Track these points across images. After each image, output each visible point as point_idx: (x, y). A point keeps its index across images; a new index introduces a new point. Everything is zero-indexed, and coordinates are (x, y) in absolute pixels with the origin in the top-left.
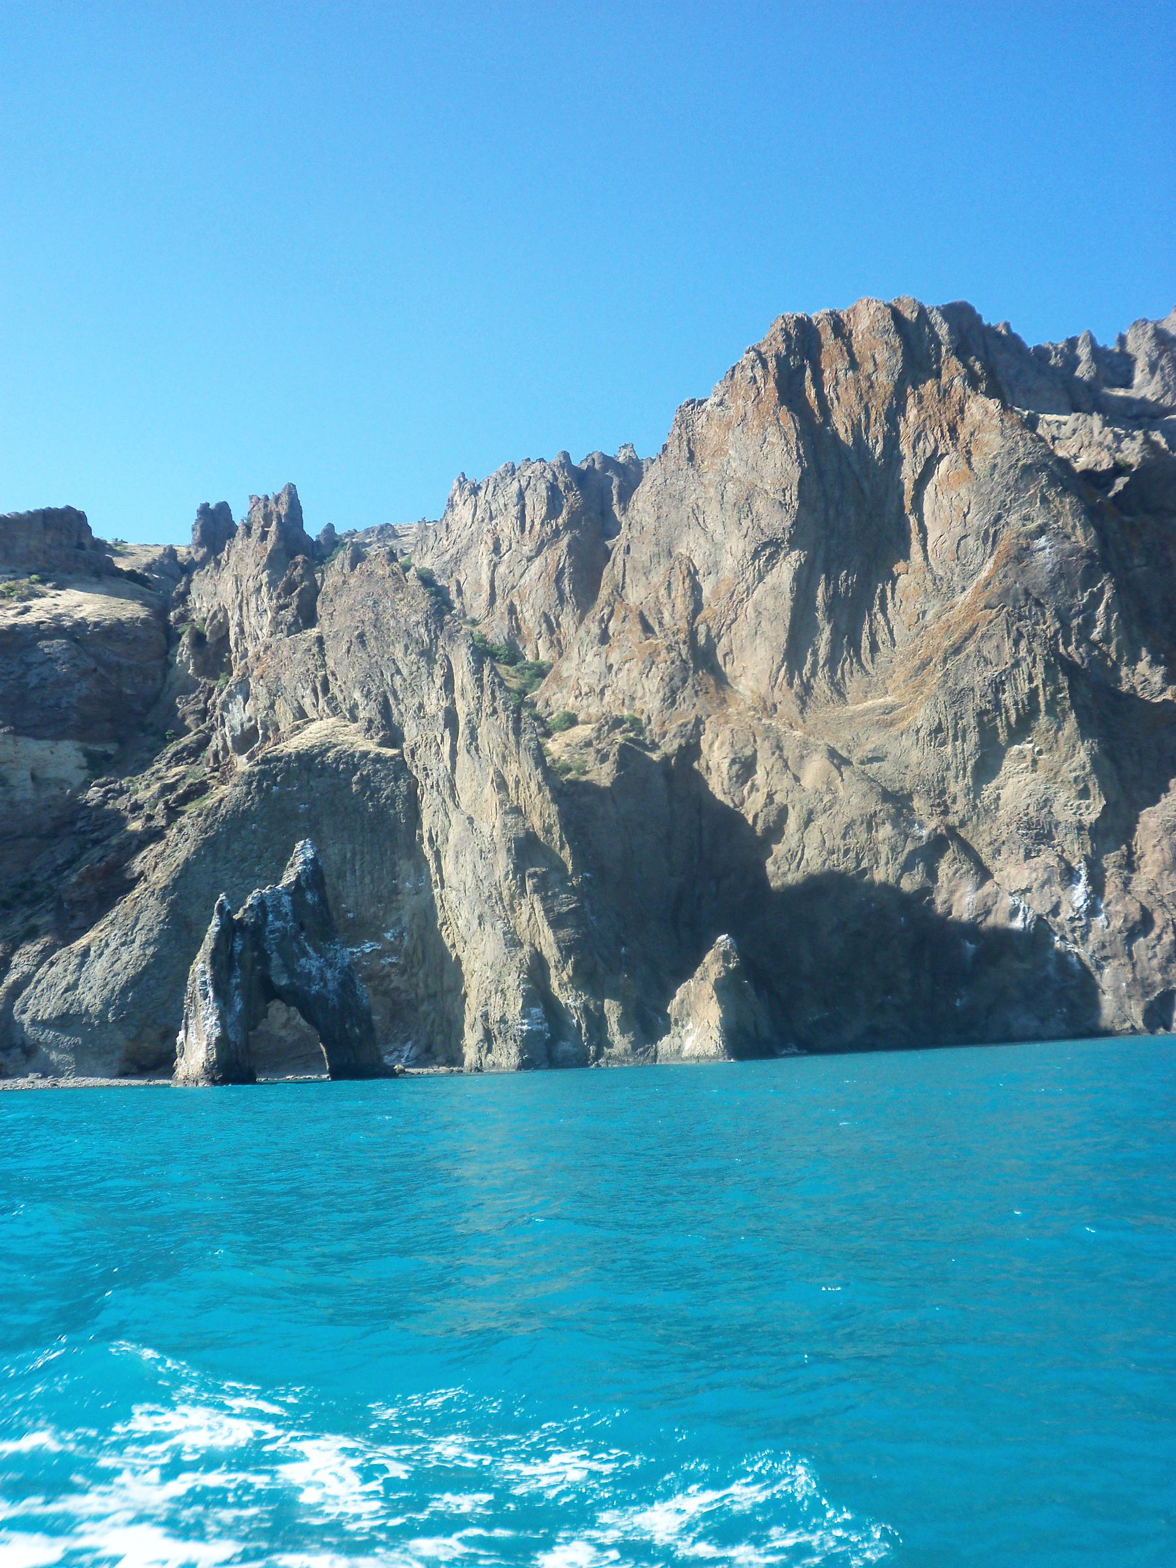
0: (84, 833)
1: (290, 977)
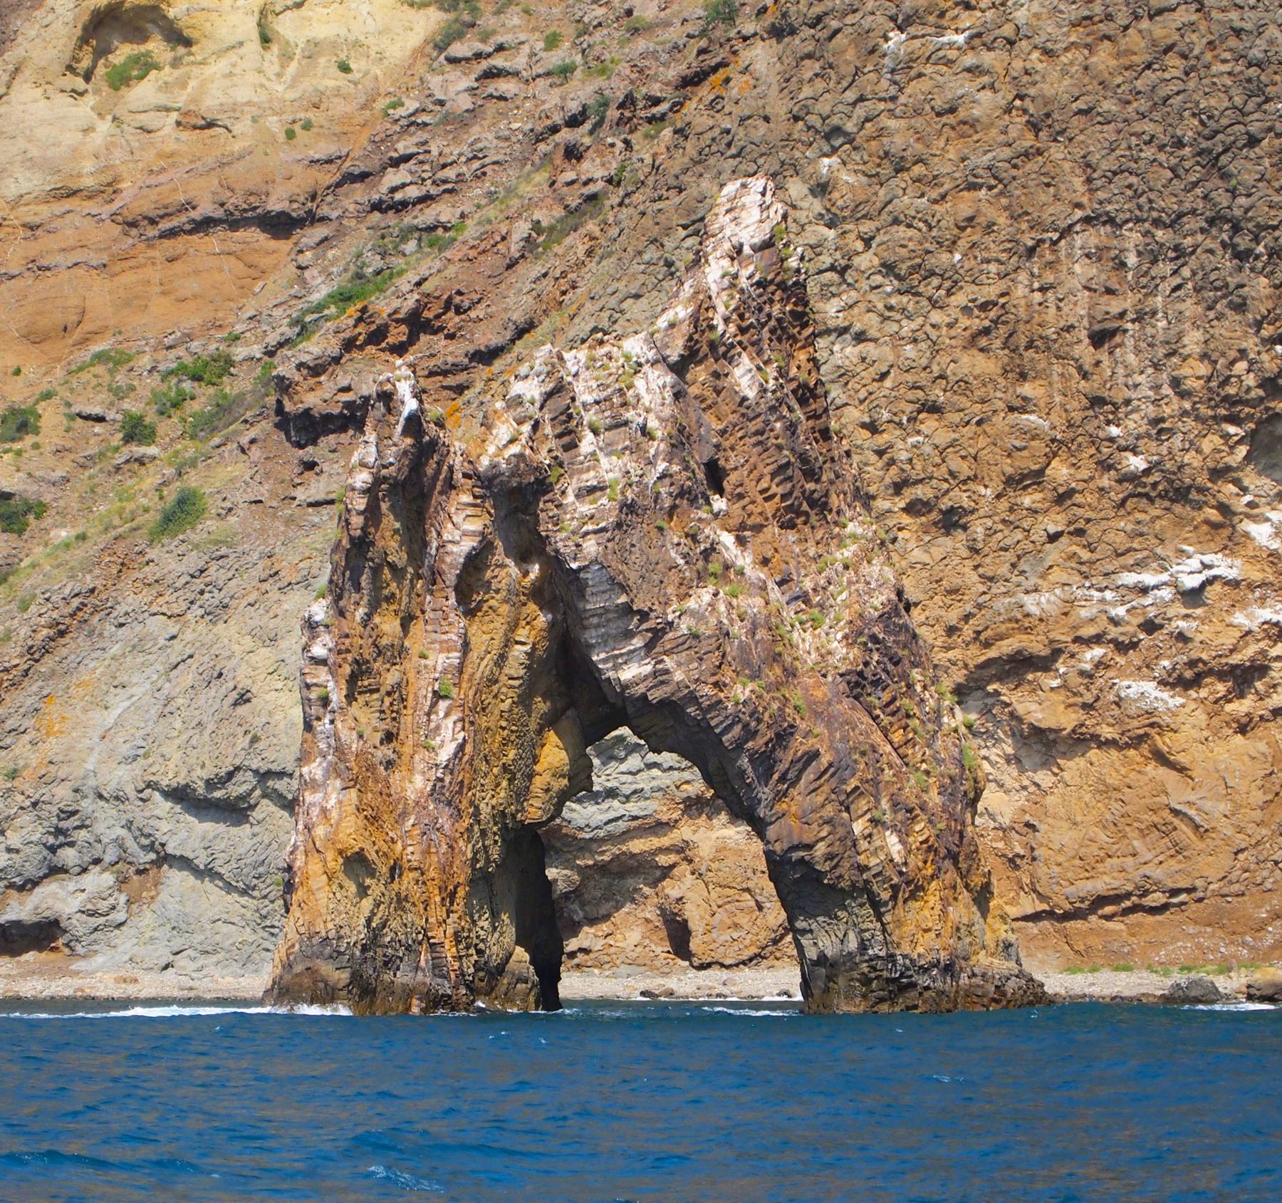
0: (403, 206)
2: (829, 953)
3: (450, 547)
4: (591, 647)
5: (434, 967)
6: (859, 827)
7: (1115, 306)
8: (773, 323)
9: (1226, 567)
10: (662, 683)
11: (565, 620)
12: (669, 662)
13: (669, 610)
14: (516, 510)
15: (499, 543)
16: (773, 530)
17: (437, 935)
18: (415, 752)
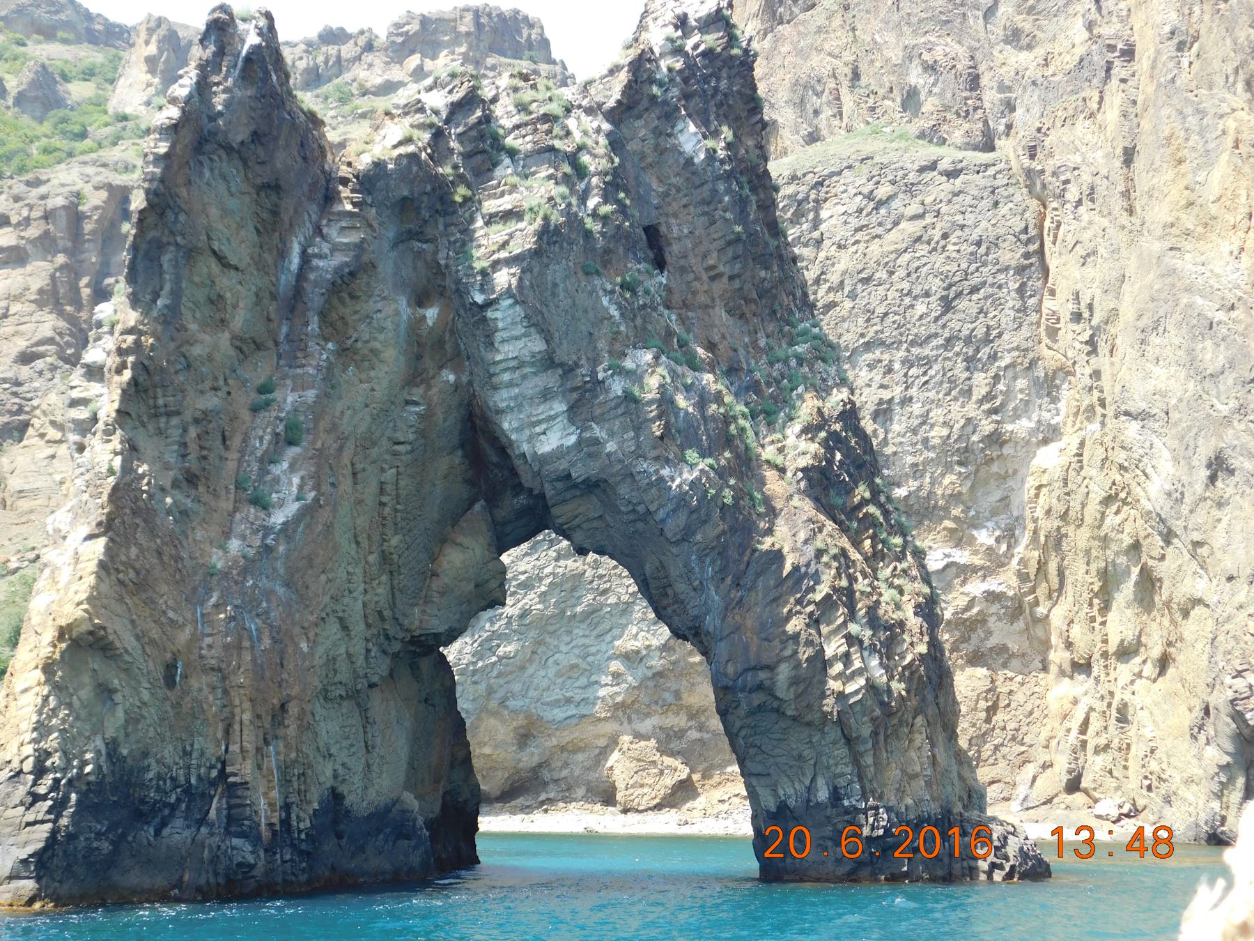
1: (574, 413)
2: (792, 803)
3: (316, 262)
4: (500, 412)
5: (231, 819)
6: (834, 647)
7: (886, 395)
8: (719, 97)
9: (962, 557)
10: (590, 455)
11: (470, 383)
13: (600, 368)
14: (412, 235)
15: (386, 268)
16: (720, 314)
17: (244, 770)
18: (236, 510)
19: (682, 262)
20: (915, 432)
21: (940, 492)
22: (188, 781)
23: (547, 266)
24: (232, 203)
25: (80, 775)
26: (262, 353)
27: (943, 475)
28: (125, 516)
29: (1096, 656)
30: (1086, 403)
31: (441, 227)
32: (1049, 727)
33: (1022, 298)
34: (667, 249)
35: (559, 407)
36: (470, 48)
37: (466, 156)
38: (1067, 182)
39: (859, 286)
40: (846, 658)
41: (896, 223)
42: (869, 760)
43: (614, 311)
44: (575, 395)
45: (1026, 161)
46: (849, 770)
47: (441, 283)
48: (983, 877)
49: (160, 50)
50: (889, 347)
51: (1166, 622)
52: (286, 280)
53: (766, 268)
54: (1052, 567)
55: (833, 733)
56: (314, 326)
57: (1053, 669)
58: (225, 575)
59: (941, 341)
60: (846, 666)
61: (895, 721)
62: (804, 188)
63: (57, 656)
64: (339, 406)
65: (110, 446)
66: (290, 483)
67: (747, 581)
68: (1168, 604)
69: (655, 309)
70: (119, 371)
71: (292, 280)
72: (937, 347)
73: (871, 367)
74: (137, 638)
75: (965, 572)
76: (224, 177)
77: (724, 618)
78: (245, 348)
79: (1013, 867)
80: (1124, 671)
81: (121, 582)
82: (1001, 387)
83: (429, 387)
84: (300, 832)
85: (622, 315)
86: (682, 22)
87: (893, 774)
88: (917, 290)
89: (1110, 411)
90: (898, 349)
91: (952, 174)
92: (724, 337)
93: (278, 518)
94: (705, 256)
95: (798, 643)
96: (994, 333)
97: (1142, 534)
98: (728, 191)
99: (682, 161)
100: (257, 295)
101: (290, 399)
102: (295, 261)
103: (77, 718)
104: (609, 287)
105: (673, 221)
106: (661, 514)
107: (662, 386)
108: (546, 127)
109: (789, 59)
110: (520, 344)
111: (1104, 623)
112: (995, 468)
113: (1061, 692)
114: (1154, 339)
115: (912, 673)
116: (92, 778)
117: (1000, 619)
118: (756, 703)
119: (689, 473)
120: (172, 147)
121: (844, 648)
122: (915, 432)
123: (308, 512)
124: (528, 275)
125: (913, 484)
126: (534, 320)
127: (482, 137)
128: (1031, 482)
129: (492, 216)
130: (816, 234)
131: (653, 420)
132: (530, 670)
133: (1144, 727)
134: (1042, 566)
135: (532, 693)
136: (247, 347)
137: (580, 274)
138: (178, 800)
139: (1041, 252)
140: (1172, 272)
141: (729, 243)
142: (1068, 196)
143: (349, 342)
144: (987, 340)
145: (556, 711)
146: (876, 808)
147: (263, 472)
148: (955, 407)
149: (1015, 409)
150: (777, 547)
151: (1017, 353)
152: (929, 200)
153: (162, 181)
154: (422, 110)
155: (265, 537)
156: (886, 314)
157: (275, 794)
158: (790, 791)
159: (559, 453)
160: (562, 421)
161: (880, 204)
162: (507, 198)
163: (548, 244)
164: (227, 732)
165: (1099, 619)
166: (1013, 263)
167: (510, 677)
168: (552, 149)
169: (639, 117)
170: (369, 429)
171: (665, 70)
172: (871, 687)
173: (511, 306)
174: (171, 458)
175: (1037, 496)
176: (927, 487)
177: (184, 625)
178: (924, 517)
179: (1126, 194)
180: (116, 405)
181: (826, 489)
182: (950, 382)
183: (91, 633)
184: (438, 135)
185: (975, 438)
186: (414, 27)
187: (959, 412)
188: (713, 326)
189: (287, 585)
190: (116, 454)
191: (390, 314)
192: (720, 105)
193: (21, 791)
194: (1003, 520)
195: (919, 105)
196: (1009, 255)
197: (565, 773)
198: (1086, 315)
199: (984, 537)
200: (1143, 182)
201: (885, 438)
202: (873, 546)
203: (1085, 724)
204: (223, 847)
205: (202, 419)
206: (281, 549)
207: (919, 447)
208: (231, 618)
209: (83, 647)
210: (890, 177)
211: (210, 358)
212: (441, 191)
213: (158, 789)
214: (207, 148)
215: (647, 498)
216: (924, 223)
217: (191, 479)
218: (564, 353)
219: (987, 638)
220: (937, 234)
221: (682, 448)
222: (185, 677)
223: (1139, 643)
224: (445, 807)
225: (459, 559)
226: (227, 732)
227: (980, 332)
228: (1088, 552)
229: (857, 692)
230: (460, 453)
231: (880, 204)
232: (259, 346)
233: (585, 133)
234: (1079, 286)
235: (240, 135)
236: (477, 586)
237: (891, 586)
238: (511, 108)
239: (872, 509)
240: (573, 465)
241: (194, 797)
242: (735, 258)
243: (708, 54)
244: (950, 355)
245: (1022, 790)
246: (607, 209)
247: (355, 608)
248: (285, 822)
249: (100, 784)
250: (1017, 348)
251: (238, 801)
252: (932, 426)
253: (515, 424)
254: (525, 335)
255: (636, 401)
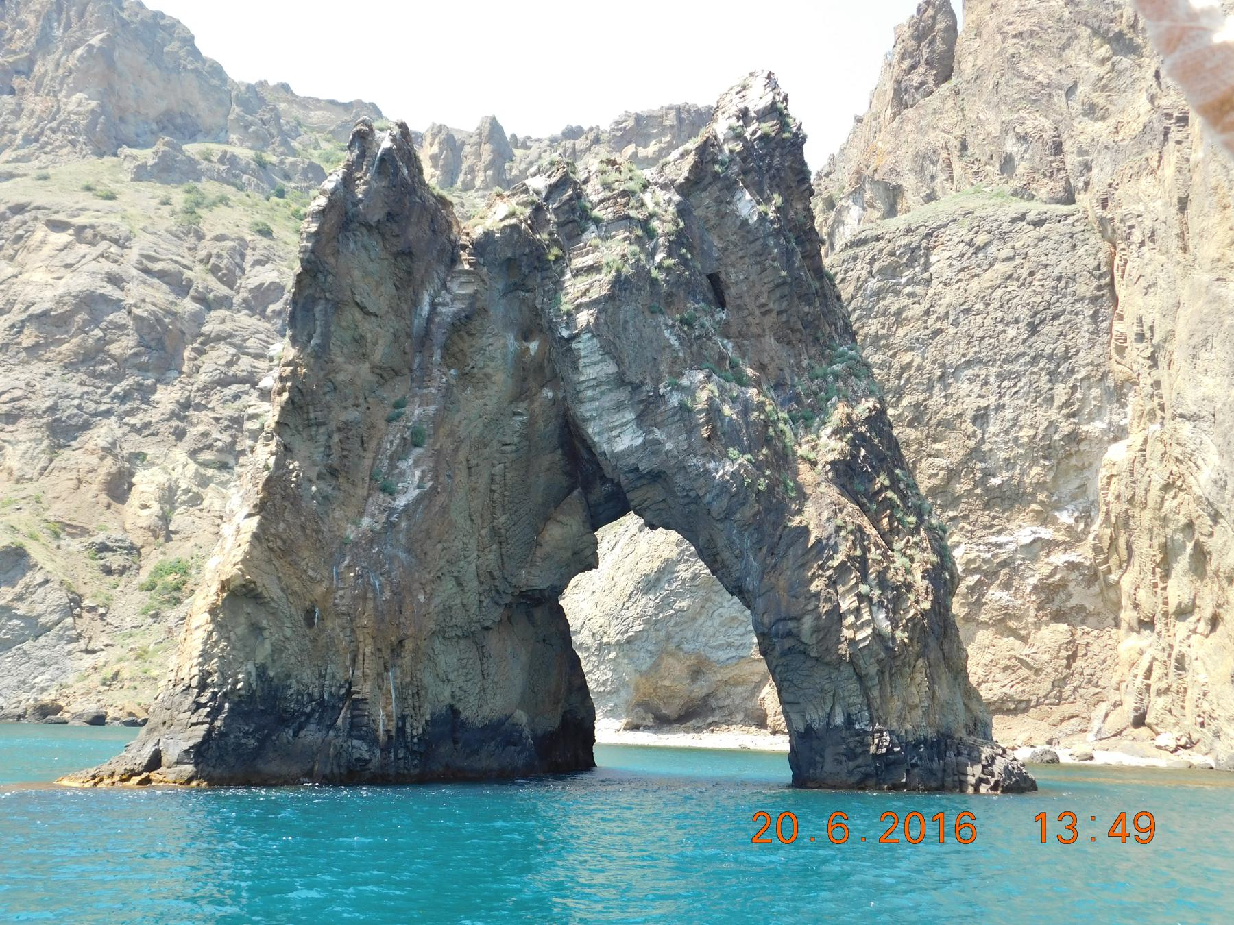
1: (642, 420)
2: (816, 726)
3: (440, 309)
4: (585, 420)
7: (983, 403)
9: (1046, 533)
11: (564, 398)
12: (658, 434)
13: (661, 386)
14: (518, 287)
15: (498, 311)
16: (770, 341)
17: (365, 689)
18: (369, 495)
19: (739, 302)
20: (1007, 432)
21: (1028, 481)
22: (322, 696)
23: (619, 307)
24: (372, 267)
25: (233, 690)
26: (398, 378)
27: (1030, 467)
28: (276, 499)
29: (1159, 615)
30: (1147, 408)
31: (539, 280)
32: (1119, 673)
33: (1095, 322)
34: (727, 292)
35: (629, 416)
36: (673, 138)
37: (560, 225)
38: (1132, 227)
39: (961, 315)
40: (857, 612)
41: (991, 265)
42: (875, 693)
43: (674, 342)
44: (641, 407)
45: (1099, 211)
46: (859, 700)
47: (536, 323)
48: (971, 790)
49: (441, 150)
50: (985, 364)
51: (1216, 587)
52: (418, 324)
53: (810, 305)
54: (1122, 542)
55: (847, 671)
56: (437, 357)
57: (1124, 625)
58: (356, 544)
59: (1028, 359)
60: (857, 618)
61: (899, 663)
62: (917, 239)
63: (220, 603)
64: (458, 417)
65: (268, 449)
66: (414, 475)
67: (780, 550)
68: (1216, 573)
69: (710, 339)
70: (280, 394)
71: (423, 322)
72: (1025, 364)
73: (971, 380)
74: (283, 590)
75: (1050, 546)
76: (365, 247)
77: (761, 580)
78: (385, 375)
79: (997, 782)
80: (1182, 628)
81: (271, 549)
82: (1078, 395)
83: (532, 402)
84: (413, 737)
85: (681, 344)
86: (744, 115)
87: (896, 704)
88: (1009, 318)
89: (1168, 414)
90: (993, 366)
91: (1037, 224)
92: (772, 359)
93: (401, 502)
94: (757, 296)
95: (819, 600)
96: (1072, 351)
97: (1194, 515)
98: (777, 245)
99: (738, 223)
100: (394, 335)
101: (416, 412)
102: (426, 308)
103: (234, 648)
104: (670, 322)
105: (731, 269)
106: (708, 498)
107: (710, 399)
108: (624, 200)
109: (912, 136)
110: (598, 368)
111: (1164, 589)
112: (1073, 461)
113: (1130, 644)
114: (1204, 355)
115: (915, 625)
116: (242, 692)
117: (1078, 584)
118: (787, 647)
119: (730, 465)
120: (321, 227)
121: (856, 604)
122: (1007, 432)
123: (425, 498)
124: (603, 315)
125: (1006, 475)
126: (607, 349)
127: (573, 210)
128: (1104, 473)
129: (578, 270)
130: (926, 275)
131: (702, 425)
132: (700, 621)
133: (1198, 674)
134: (1113, 541)
135: (702, 639)
136: (386, 374)
137: (647, 313)
138: (313, 710)
139: (1111, 284)
140: (1217, 299)
141: (777, 286)
142: (1133, 238)
143: (468, 369)
144: (1066, 358)
145: (720, 653)
146: (881, 732)
147: (392, 466)
148: (1040, 412)
149: (1090, 413)
150: (804, 523)
151: (1090, 368)
152: (1018, 245)
153: (313, 252)
154: (526, 191)
155: (389, 516)
156: (983, 338)
157: (393, 708)
158: (815, 717)
159: (630, 451)
160: (632, 426)
161: (979, 249)
162: (590, 256)
163: (620, 290)
164: (354, 660)
165: (1161, 585)
166: (1088, 294)
167: (684, 626)
168: (627, 217)
169: (705, 189)
170: (482, 435)
171: (727, 152)
172: (877, 635)
173: (590, 339)
174: (318, 457)
175: (1109, 484)
176: (1017, 477)
177: (321, 581)
178: (1015, 501)
179: (1181, 236)
180: (276, 419)
181: (851, 478)
182: (1036, 392)
183: (244, 586)
184: (538, 209)
185: (1056, 437)
186: (630, 123)
187: (1043, 416)
188: (763, 351)
189: (408, 551)
190: (272, 454)
191: (499, 346)
192: (773, 178)
193: (190, 700)
194: (1081, 504)
195: (1014, 168)
196: (1084, 288)
197: (728, 702)
198: (1148, 335)
199: (1065, 518)
200: (1195, 225)
201: (983, 438)
202: (890, 523)
203: (1149, 672)
204: (345, 746)
205: (344, 428)
206: (403, 524)
207: (1010, 444)
208: (358, 577)
209: (239, 596)
210: (987, 228)
211: (352, 382)
212: (538, 252)
213: (297, 702)
214: (352, 226)
215: (697, 485)
216: (1013, 263)
217: (333, 473)
218: (631, 376)
219: (1067, 600)
220: (1024, 272)
221: (726, 446)
222: (322, 619)
223: (1194, 605)
224: (564, 722)
225: (557, 533)
226: (354, 660)
227: (1060, 351)
228: (1151, 530)
229: (865, 639)
230: (560, 451)
231: (979, 249)
232: (396, 373)
233: (657, 204)
234: (1142, 312)
235: (376, 216)
236: (575, 553)
237: (904, 555)
238: (598, 187)
239: (890, 494)
240: (640, 461)
241: (325, 709)
242: (783, 297)
243: (764, 138)
244: (1036, 370)
245: (1096, 724)
246: (670, 262)
247: (469, 570)
248: (401, 730)
249: (251, 697)
250: (1091, 364)
251: (358, 712)
252: (1021, 427)
253: (597, 429)
254: (602, 361)
255: (690, 410)
